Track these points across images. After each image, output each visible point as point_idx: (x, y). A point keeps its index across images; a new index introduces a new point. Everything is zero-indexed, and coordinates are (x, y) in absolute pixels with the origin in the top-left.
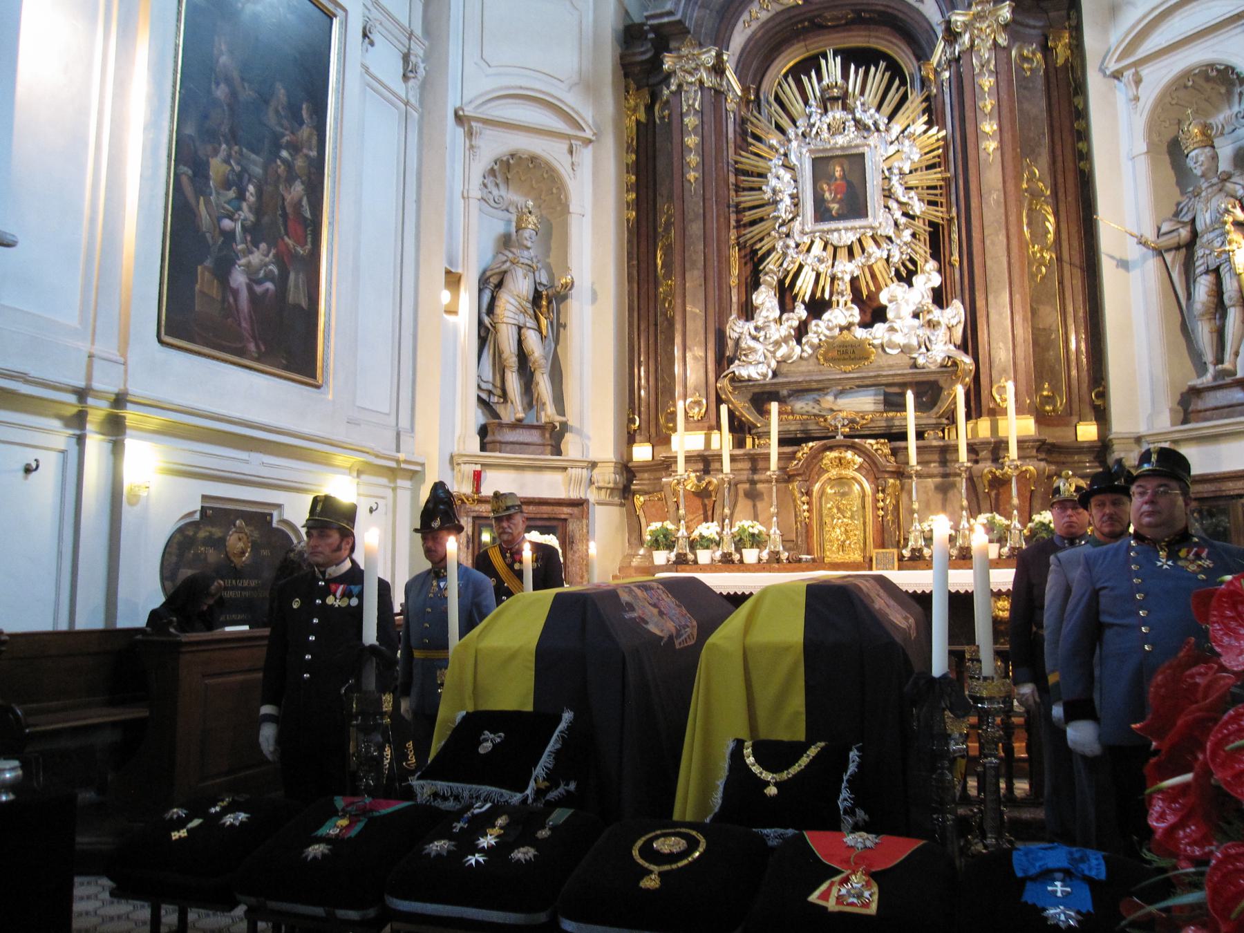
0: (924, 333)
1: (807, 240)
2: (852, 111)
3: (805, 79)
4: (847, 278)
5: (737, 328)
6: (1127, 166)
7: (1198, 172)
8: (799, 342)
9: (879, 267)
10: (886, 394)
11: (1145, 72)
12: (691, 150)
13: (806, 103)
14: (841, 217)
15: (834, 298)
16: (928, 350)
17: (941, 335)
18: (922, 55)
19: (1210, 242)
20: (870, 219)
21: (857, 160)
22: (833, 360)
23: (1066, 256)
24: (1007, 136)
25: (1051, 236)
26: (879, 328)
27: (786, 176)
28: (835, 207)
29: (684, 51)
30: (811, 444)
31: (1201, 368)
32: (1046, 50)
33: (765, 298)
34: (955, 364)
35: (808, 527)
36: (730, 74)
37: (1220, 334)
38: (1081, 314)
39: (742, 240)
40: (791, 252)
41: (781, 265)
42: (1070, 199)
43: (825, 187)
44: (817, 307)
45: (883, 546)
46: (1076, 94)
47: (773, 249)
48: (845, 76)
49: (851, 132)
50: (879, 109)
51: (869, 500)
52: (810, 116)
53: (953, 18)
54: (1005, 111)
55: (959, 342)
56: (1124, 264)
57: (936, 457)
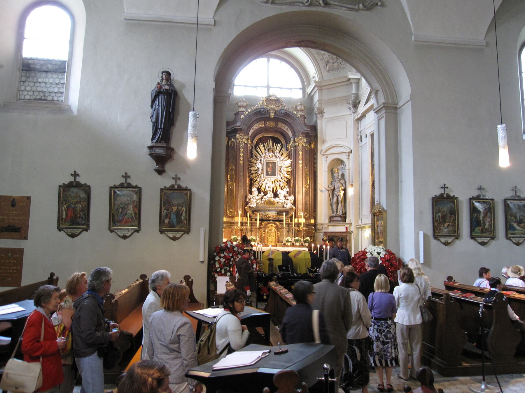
0: (286, 201)
1: (264, 179)
2: (274, 153)
3: (265, 144)
4: (272, 188)
5: (250, 196)
6: (324, 173)
7: (336, 177)
8: (261, 200)
9: (278, 186)
10: (278, 212)
11: (328, 156)
12: (241, 156)
13: (265, 150)
14: (270, 175)
15: (269, 192)
16: (287, 204)
17: (289, 202)
18: (287, 143)
19: (337, 191)
20: (277, 176)
21: (274, 164)
22: (268, 204)
23: (311, 187)
24: (304, 164)
25: (308, 183)
26: (277, 198)
27: (260, 165)
28: (270, 173)
29: (241, 134)
30: (265, 222)
31: (333, 212)
32: (310, 145)
33: (254, 189)
34: (292, 208)
35: (264, 239)
36: (249, 140)
37: (337, 207)
38: (313, 198)
39: (251, 177)
40: (261, 181)
41: (259, 183)
42: (312, 176)
43: (268, 168)
44: (266, 193)
45: (278, 242)
46: (315, 155)
47: (257, 180)
48: (273, 146)
49: (274, 157)
50: (279, 153)
51: (276, 233)
52: (266, 153)
53: (296, 139)
54: (304, 160)
55: (292, 203)
56: (321, 191)
57: (287, 225)
